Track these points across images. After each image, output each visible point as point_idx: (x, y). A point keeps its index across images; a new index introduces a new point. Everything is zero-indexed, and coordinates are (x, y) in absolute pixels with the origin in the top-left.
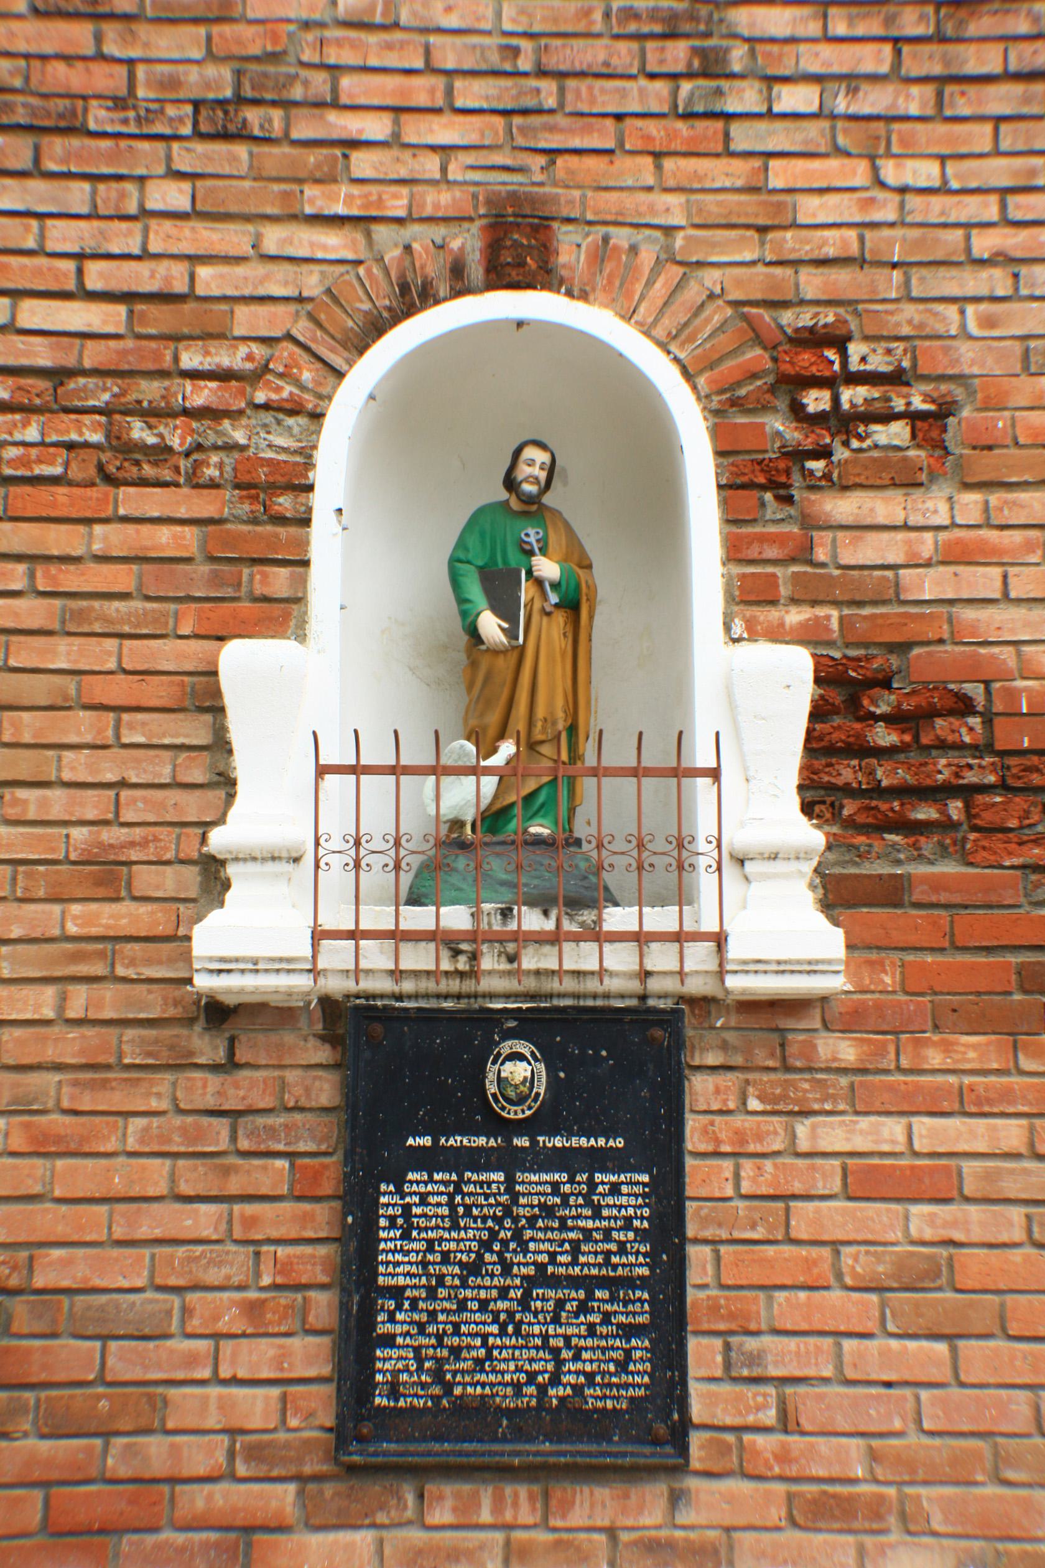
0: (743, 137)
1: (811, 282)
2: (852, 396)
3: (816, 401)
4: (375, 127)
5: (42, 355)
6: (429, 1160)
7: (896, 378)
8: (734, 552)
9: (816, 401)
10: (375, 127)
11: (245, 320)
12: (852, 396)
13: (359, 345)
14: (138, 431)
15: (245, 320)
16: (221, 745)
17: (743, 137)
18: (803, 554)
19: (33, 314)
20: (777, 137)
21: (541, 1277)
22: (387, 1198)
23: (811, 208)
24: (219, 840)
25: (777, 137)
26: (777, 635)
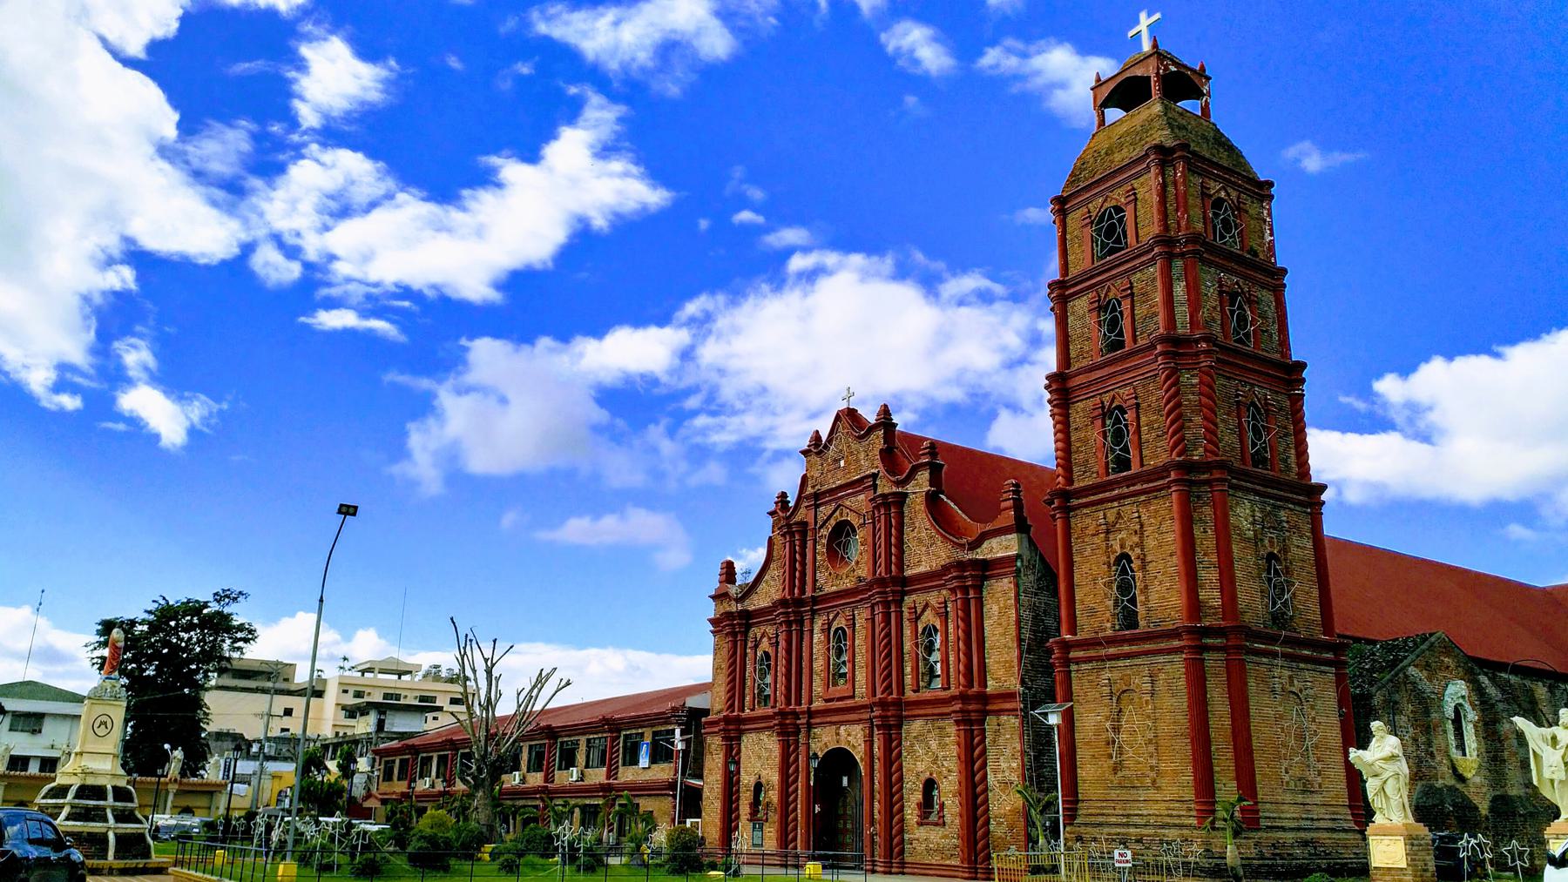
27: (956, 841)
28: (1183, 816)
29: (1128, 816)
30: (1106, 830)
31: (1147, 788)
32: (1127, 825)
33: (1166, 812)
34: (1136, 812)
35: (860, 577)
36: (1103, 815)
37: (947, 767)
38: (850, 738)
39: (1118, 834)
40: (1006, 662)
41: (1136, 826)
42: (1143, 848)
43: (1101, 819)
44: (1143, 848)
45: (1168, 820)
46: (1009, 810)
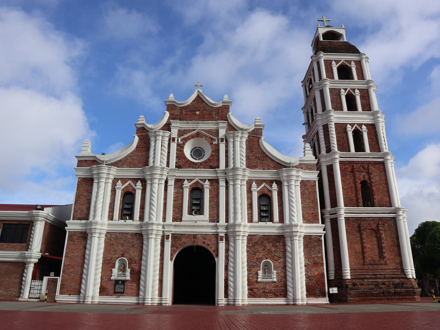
0: (130, 252)
1: (132, 257)
2: (133, 261)
3: (131, 261)
4: (118, 252)
5: (108, 259)
6: (117, 285)
7: (134, 260)
8: (128, 266)
9: (131, 261)
10: (118, 252)
11: (114, 258)
12: (133, 261)
13: (117, 259)
14: (110, 262)
15: (114, 258)
16: (112, 272)
17: (130, 252)
18: (130, 266)
19: (108, 258)
20: (131, 252)
21: (120, 288)
22: (116, 286)
23: (132, 255)
24: (112, 275)
25: (131, 252)
26: (129, 269)
27: (283, 288)
28: (400, 274)
29: (375, 275)
30: (366, 280)
31: (382, 265)
32: (376, 278)
33: (391, 273)
34: (379, 273)
35: (212, 166)
36: (363, 275)
37: (277, 256)
38: (205, 241)
39: (372, 282)
40: (313, 213)
41: (380, 278)
42: (386, 286)
43: (362, 277)
44: (386, 286)
45: (394, 276)
46: (317, 274)
